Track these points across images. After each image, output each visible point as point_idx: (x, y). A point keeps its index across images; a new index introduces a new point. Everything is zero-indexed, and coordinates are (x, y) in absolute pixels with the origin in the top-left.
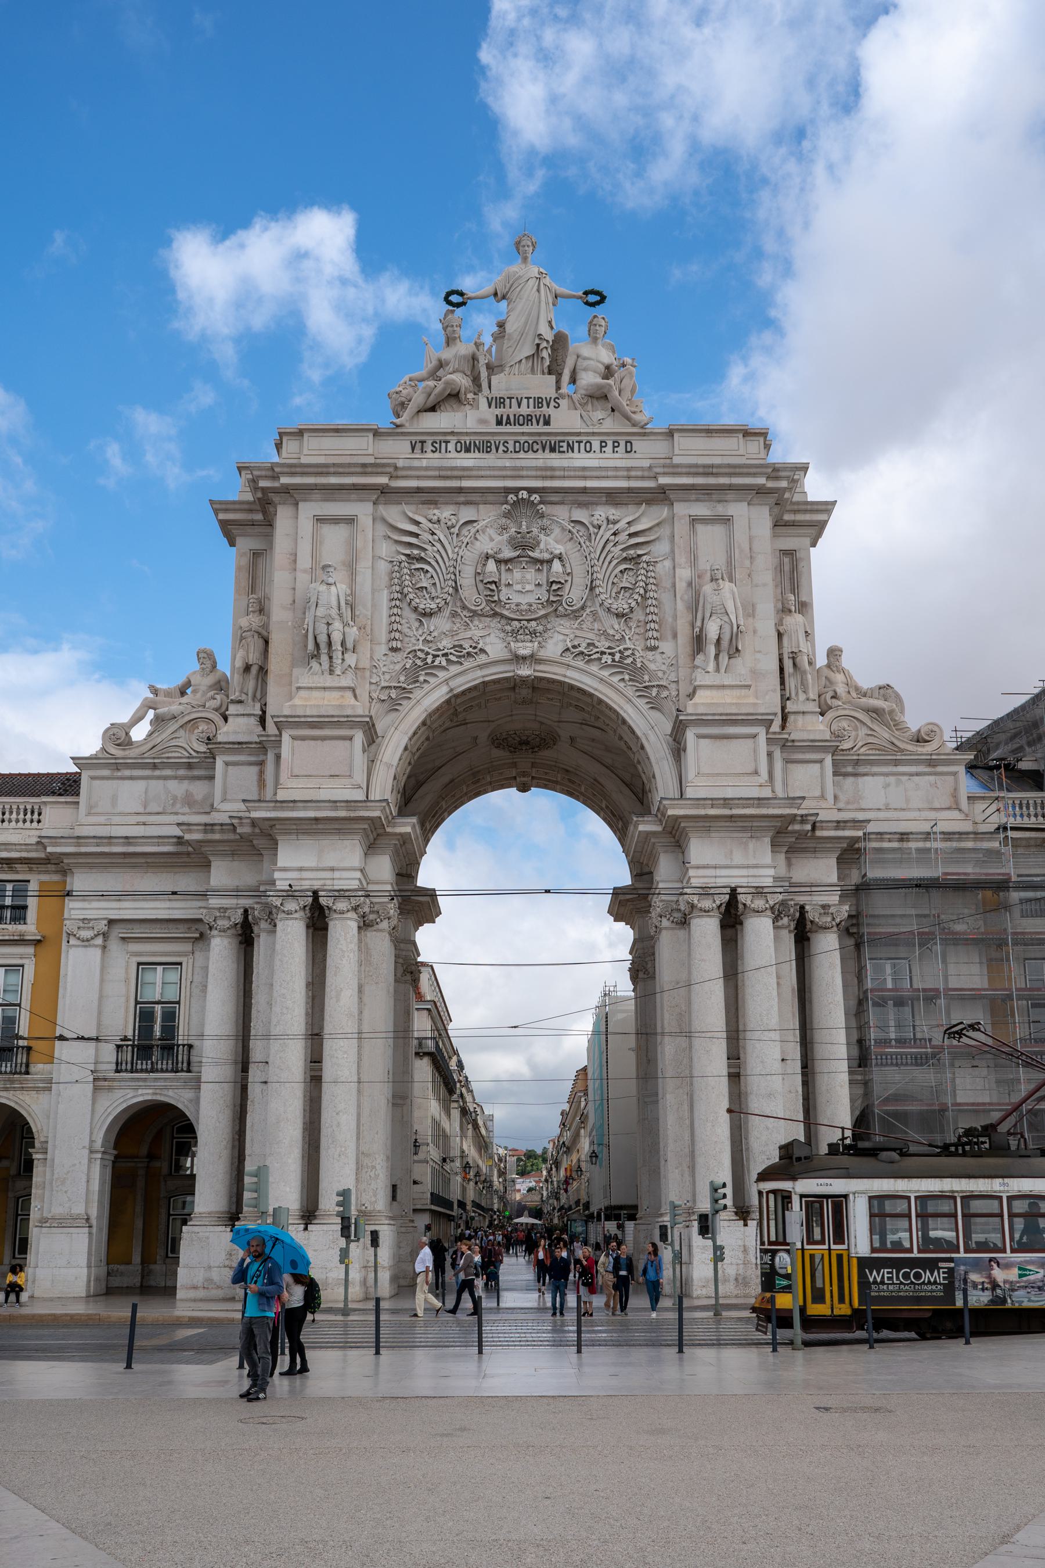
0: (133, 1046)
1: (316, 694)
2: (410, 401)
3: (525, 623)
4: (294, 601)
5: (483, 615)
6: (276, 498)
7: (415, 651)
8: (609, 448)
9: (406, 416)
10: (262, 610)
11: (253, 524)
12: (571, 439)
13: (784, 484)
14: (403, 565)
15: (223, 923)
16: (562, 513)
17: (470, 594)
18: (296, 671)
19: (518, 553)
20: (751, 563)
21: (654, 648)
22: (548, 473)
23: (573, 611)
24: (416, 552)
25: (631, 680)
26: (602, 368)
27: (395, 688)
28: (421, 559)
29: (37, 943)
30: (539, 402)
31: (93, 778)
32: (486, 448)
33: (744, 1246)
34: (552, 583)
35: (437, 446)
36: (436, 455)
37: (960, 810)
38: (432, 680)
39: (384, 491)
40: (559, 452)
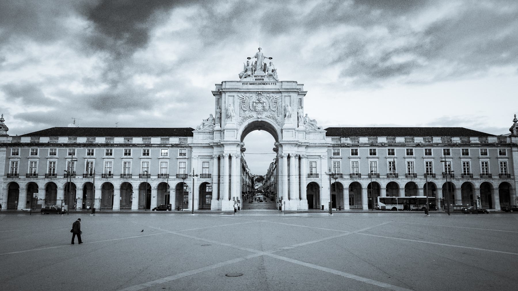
1: (229, 124)
2: (242, 76)
9: (242, 79)
10: (220, 108)
11: (218, 94)
12: (267, 83)
13: (299, 91)
15: (216, 157)
16: (265, 95)
17: (251, 108)
18: (226, 120)
19: (259, 101)
21: (279, 116)
22: (263, 89)
24: (243, 101)
26: (272, 70)
28: (244, 102)
29: (188, 159)
30: (262, 76)
31: (195, 134)
32: (254, 84)
38: (246, 121)
39: (238, 91)
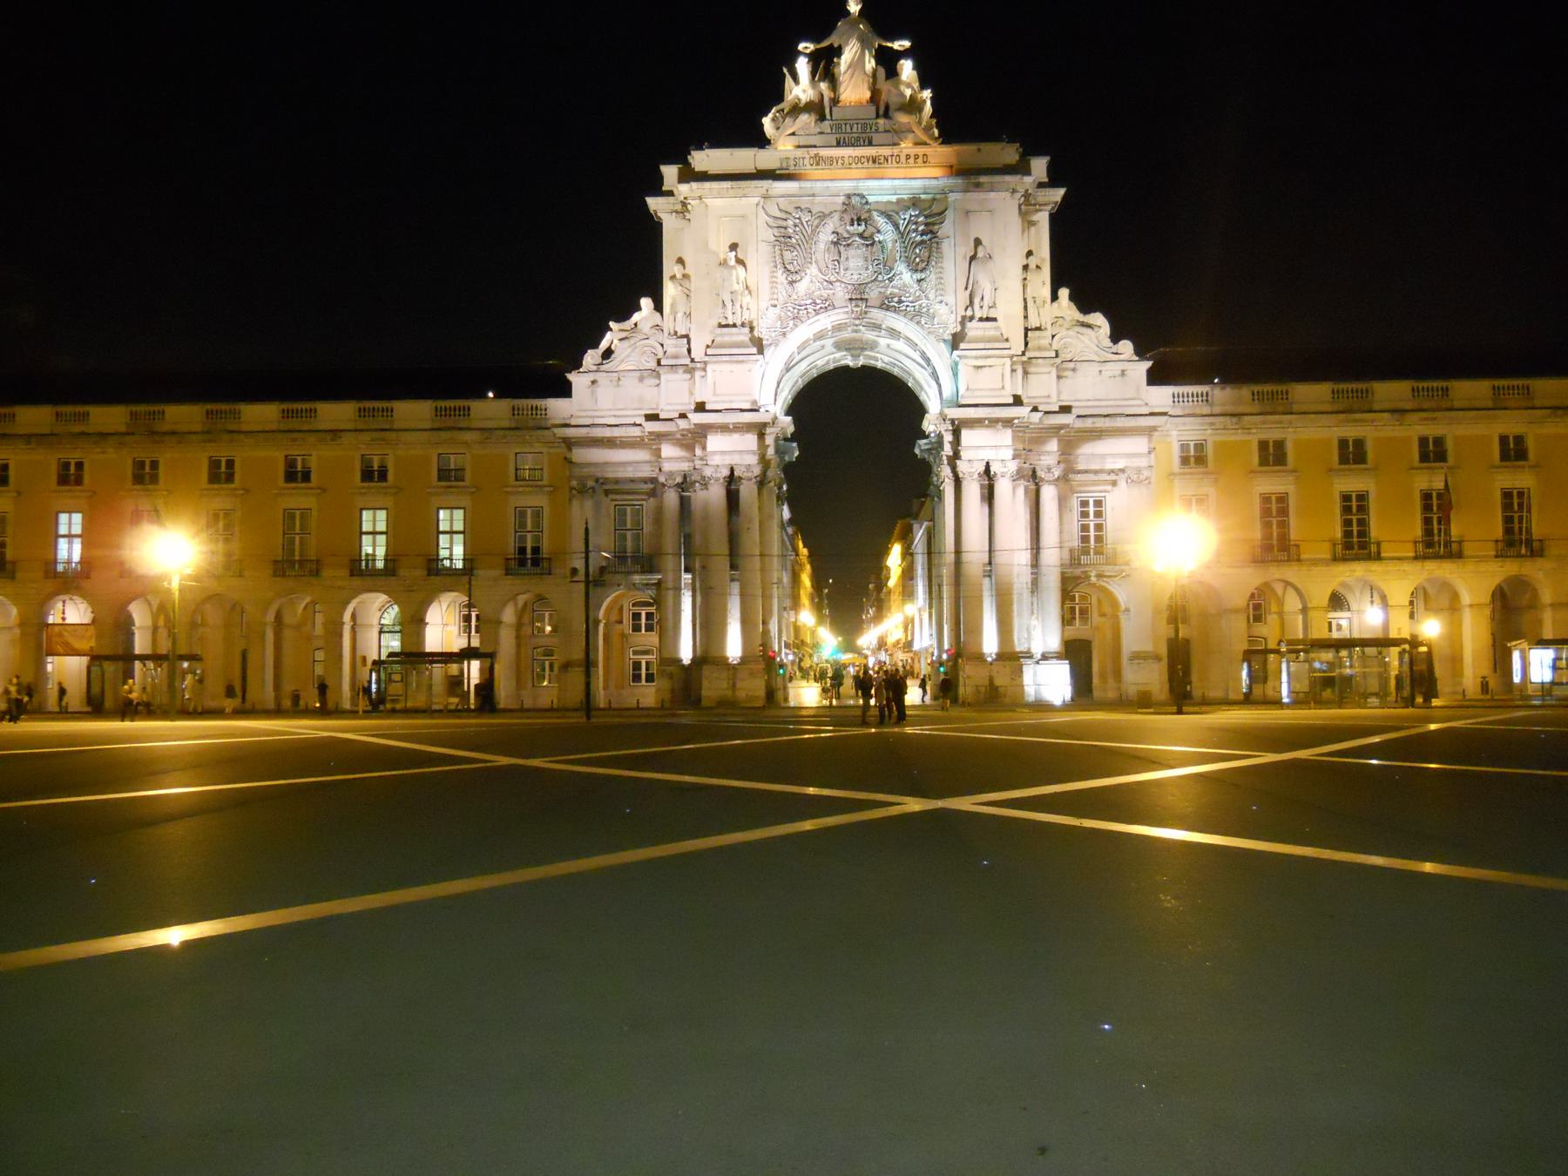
8: (912, 160)
14: (777, 248)
21: (941, 302)
23: (888, 279)
36: (797, 168)
37: (1141, 399)
40: (879, 163)
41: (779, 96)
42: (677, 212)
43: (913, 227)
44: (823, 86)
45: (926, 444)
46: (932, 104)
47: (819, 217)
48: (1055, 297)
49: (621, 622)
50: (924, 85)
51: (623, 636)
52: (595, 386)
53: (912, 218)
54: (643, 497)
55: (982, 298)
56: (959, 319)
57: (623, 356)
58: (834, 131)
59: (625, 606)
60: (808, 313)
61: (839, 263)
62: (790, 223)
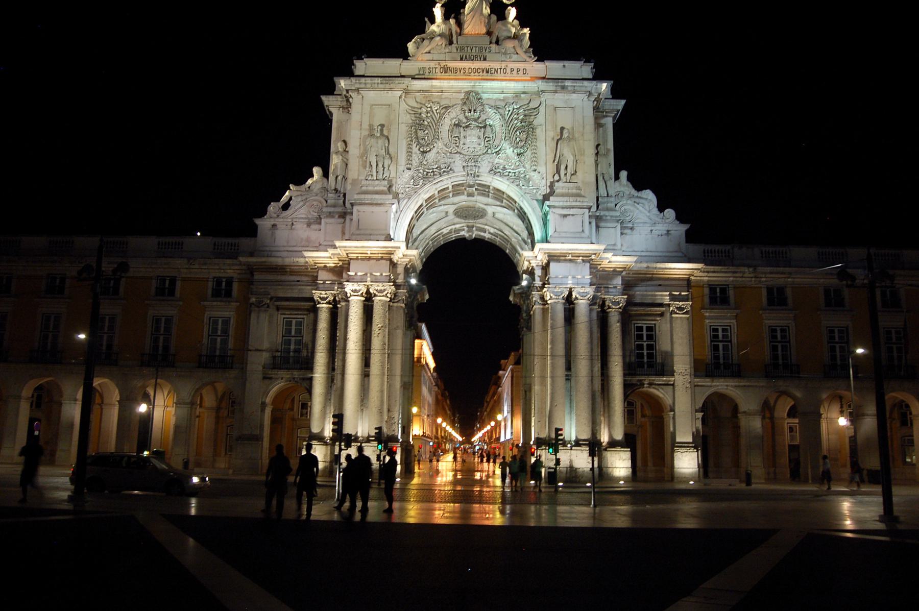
0: (280, 356)
3: (473, 157)
4: (360, 145)
5: (451, 153)
6: (354, 95)
7: (418, 170)
14: (413, 128)
20: (584, 129)
21: (535, 170)
23: (496, 152)
25: (523, 186)
27: (409, 187)
30: (481, 49)
33: (570, 459)
34: (486, 137)
35: (431, 69)
41: (423, 31)
42: (343, 108)
43: (515, 116)
44: (452, 21)
45: (519, 289)
46: (530, 38)
47: (446, 107)
48: (617, 178)
49: (292, 409)
50: (523, 26)
51: (293, 419)
52: (273, 228)
53: (515, 110)
54: (305, 313)
55: (567, 167)
56: (548, 184)
57: (296, 208)
58: (459, 51)
59: (296, 397)
60: (434, 175)
61: (459, 139)
62: (424, 110)
